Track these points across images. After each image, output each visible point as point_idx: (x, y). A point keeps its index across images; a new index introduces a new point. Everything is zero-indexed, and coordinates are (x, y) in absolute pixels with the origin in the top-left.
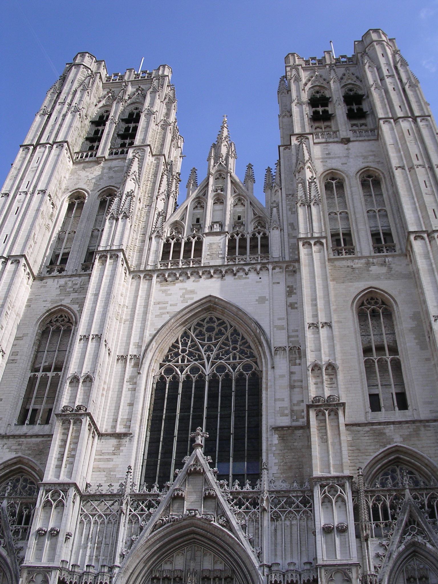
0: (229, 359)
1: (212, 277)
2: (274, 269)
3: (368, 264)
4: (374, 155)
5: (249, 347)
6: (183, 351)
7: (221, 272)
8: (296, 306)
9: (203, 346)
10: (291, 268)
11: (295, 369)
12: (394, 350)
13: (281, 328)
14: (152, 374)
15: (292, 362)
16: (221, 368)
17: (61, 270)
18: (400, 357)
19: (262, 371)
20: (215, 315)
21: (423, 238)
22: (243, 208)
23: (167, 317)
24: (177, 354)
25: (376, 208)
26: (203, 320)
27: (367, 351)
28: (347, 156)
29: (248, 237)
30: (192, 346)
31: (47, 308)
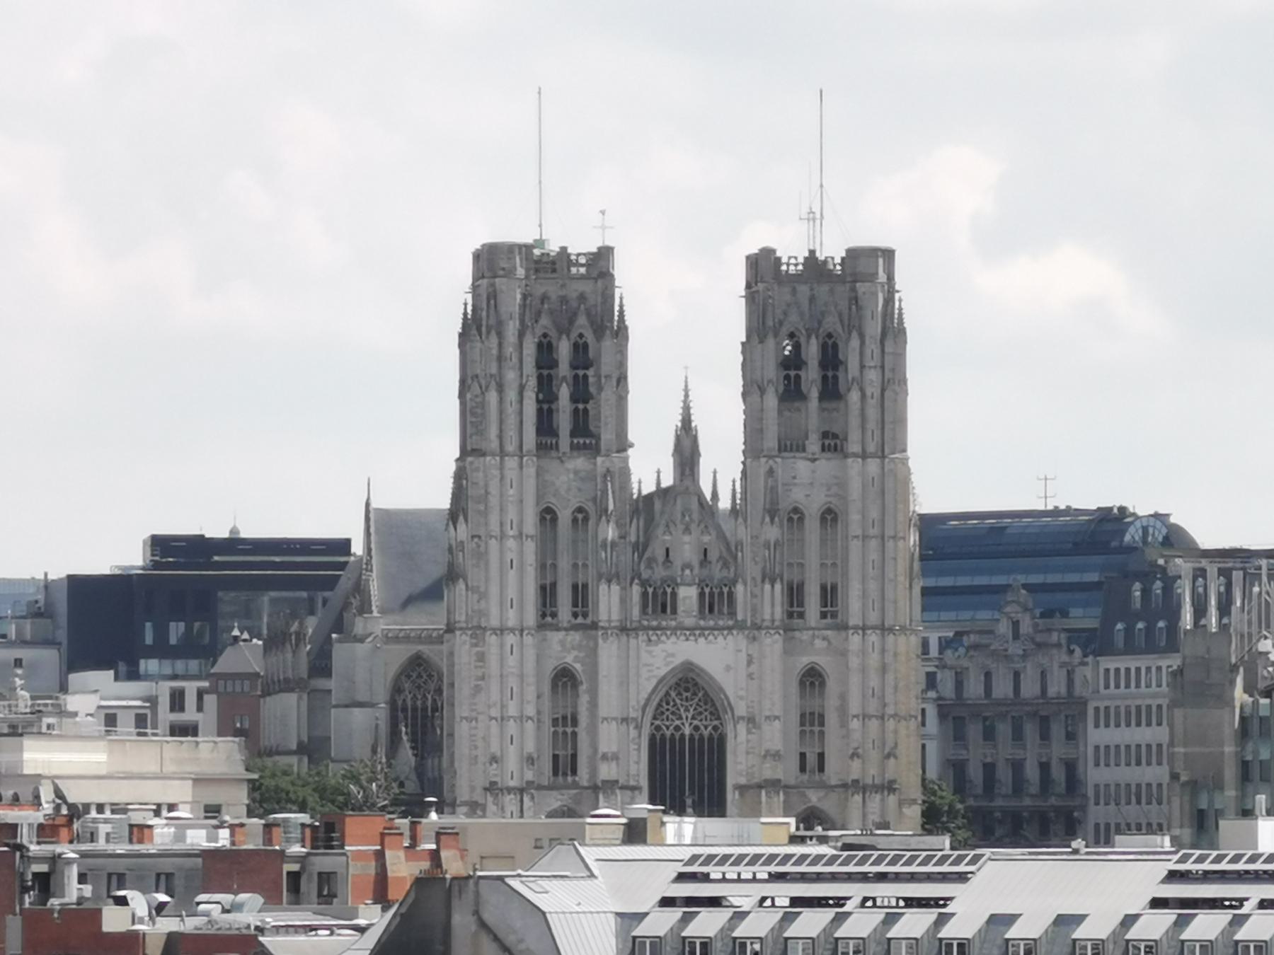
0: (701, 720)
1: (687, 640)
2: (738, 634)
3: (814, 636)
4: (837, 484)
5: (716, 709)
6: (668, 710)
7: (695, 635)
8: (754, 676)
9: (682, 705)
10: (751, 635)
11: (750, 737)
12: (822, 716)
13: (741, 698)
14: (647, 733)
15: (749, 732)
16: (696, 728)
17: (554, 615)
18: (825, 729)
19: (726, 734)
20: (691, 675)
21: (858, 634)
22: (709, 538)
23: (654, 682)
24: (663, 713)
25: (829, 562)
26: (680, 680)
27: (803, 716)
28: (811, 484)
29: (716, 591)
30: (674, 706)
31: (553, 667)
